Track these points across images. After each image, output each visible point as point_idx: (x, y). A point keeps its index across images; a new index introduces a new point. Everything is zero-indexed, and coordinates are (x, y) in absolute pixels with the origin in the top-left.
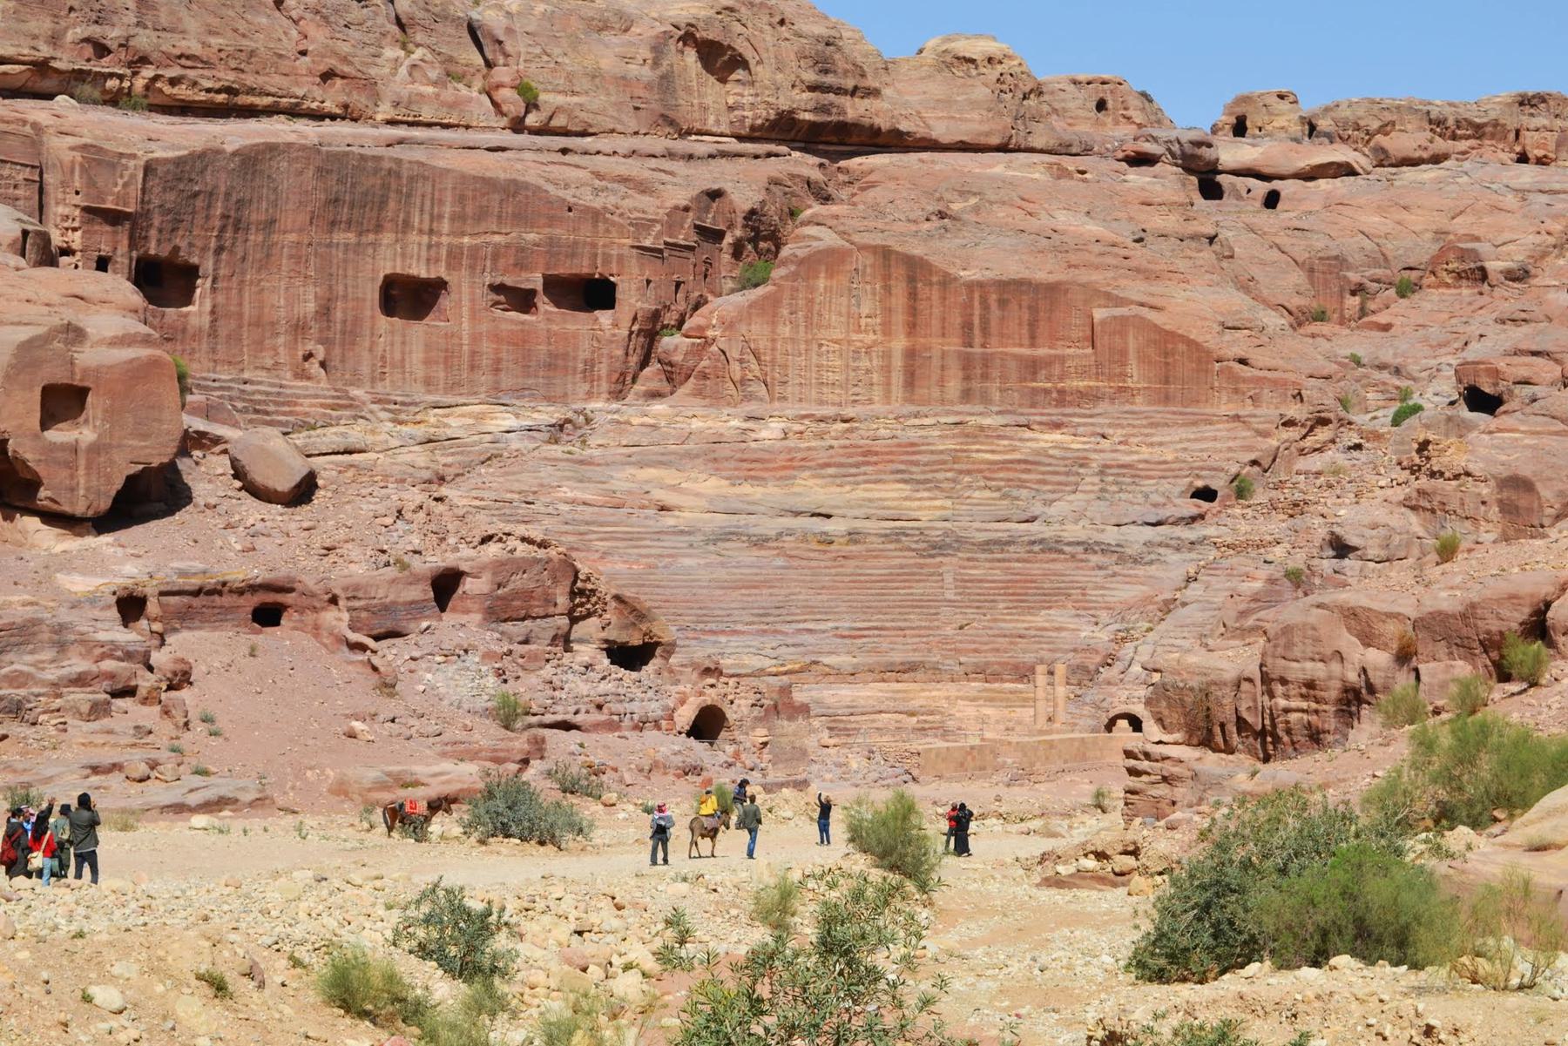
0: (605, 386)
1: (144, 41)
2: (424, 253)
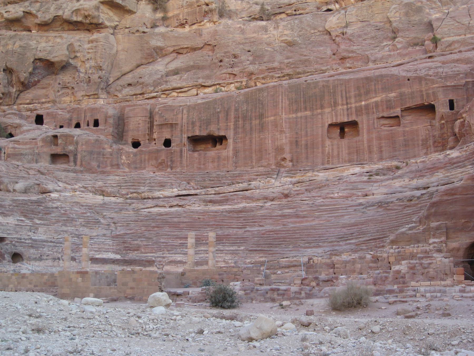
0: (432, 149)
1: (251, 68)
2: (346, 113)
